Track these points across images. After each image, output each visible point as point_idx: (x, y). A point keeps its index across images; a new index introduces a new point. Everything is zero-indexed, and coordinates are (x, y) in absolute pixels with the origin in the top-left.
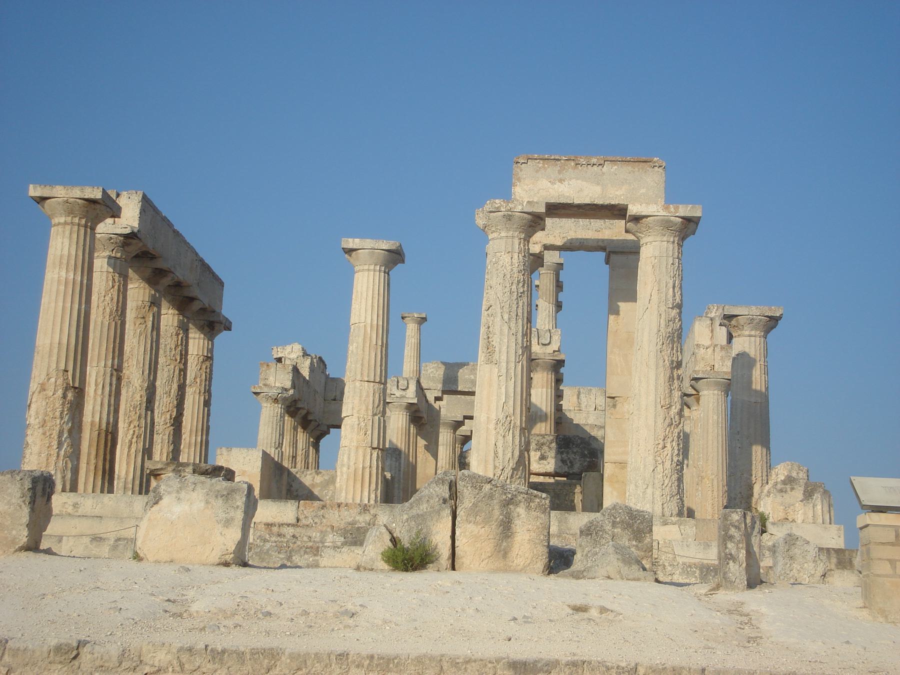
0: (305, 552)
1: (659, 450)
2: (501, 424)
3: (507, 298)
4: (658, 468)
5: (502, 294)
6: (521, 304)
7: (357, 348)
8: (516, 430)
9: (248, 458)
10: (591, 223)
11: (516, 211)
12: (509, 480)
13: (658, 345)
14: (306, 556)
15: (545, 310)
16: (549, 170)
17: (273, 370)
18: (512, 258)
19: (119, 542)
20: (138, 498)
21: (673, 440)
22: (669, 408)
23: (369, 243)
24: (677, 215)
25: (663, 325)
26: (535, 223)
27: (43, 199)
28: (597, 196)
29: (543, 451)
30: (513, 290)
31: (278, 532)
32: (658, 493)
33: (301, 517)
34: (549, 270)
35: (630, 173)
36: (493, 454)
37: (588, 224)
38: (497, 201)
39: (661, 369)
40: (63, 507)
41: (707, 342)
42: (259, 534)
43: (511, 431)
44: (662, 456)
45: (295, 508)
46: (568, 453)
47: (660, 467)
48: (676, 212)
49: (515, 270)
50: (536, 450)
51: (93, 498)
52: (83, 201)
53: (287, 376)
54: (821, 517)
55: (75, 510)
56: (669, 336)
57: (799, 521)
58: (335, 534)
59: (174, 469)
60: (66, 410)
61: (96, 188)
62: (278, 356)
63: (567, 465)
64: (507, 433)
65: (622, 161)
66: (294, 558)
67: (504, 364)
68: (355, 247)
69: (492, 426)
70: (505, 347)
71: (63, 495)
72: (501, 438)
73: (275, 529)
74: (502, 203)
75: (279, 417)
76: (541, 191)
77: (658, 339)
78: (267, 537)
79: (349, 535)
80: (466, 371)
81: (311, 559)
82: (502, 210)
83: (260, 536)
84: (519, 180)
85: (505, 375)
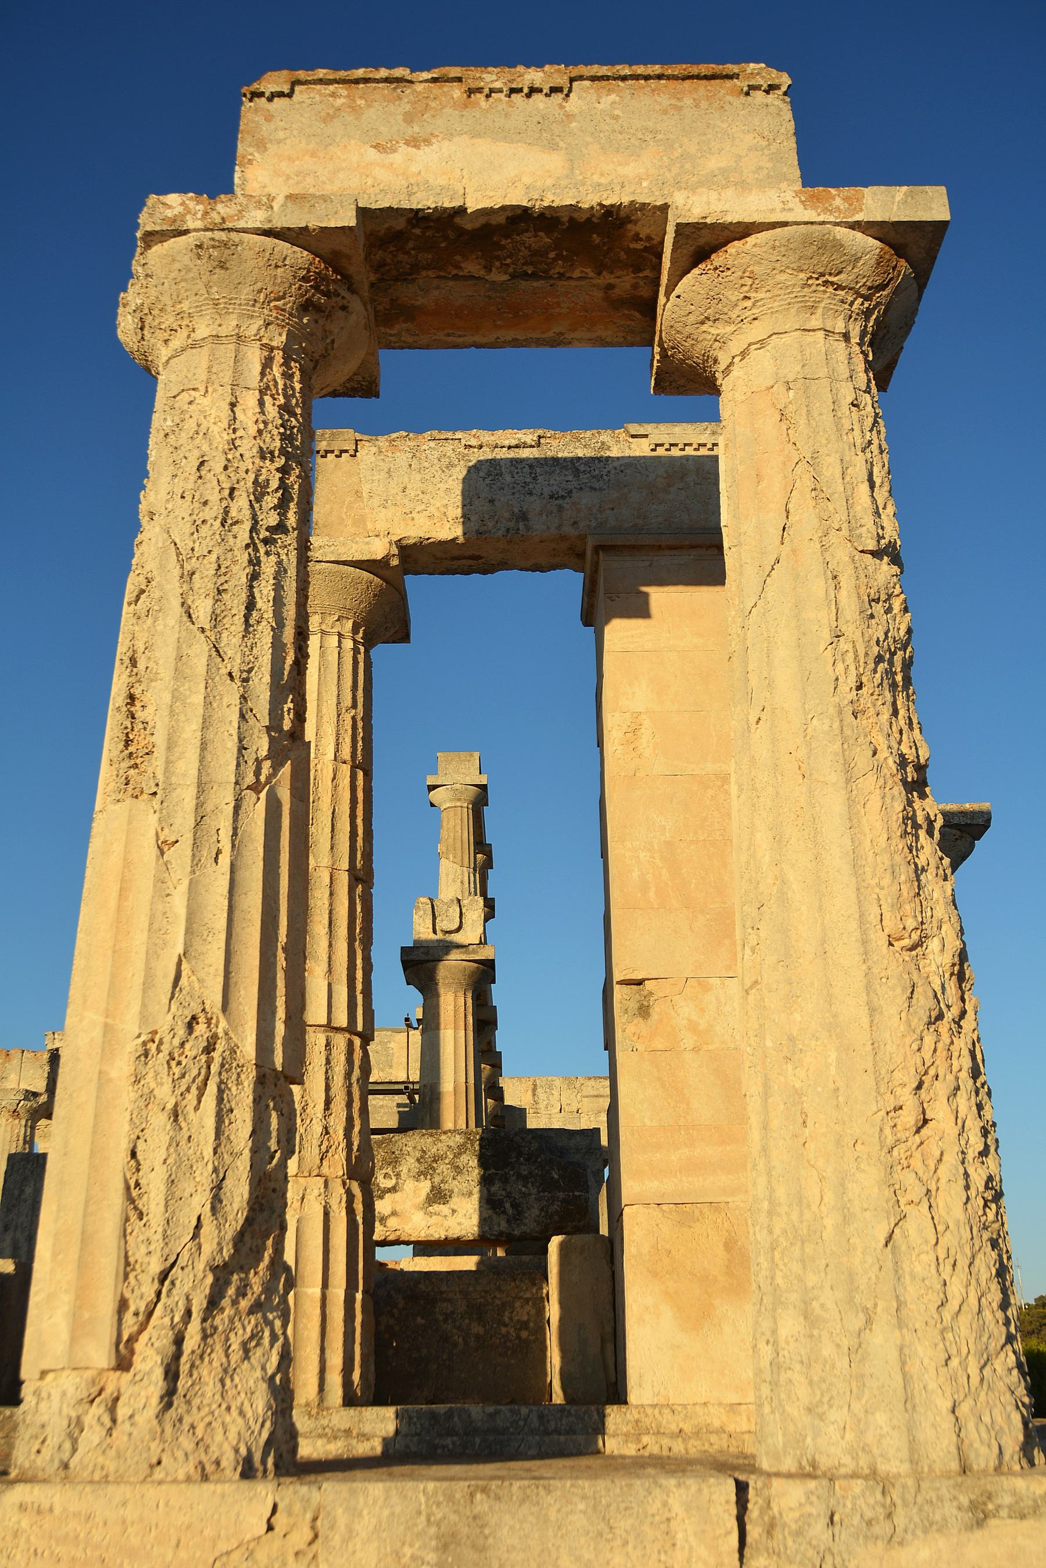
1: (902, 1135)
2: (163, 1056)
4: (910, 1226)
5: (188, 528)
6: (268, 567)
8: (239, 1083)
10: (535, 478)
11: (241, 224)
18: (233, 405)
26: (327, 294)
28: (549, 182)
29: (437, 1179)
30: (233, 513)
34: (459, 800)
35: (665, 112)
36: (116, 1199)
39: (870, 782)
43: (212, 1088)
44: (916, 1163)
46: (505, 1180)
49: (248, 447)
53: (41, 1071)
56: (879, 659)
62: (55, 1047)
63: (504, 1212)
67: (188, 796)
69: (122, 1067)
70: (195, 725)
72: (159, 1121)
75: (21, 1142)
76: (341, 175)
77: (840, 667)
84: (261, 145)
85: (189, 836)
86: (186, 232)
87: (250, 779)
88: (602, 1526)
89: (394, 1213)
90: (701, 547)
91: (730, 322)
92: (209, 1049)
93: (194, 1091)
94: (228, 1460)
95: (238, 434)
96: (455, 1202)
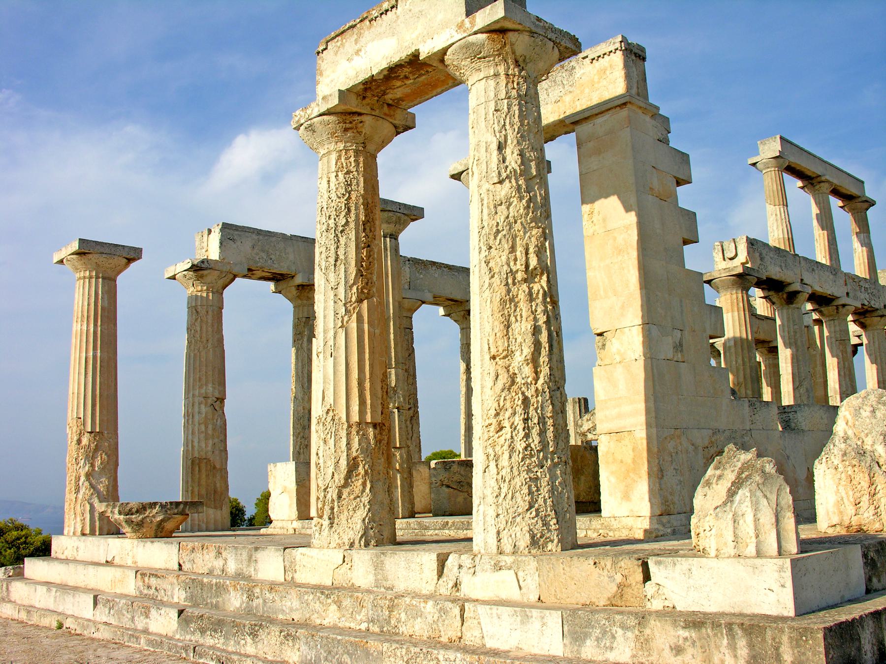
1: (491, 435)
3: (324, 239)
10: (548, 95)
11: (313, 116)
12: (336, 504)
13: (483, 251)
15: (772, 215)
18: (329, 181)
21: (515, 413)
22: (509, 354)
24: (475, 29)
25: (485, 217)
26: (351, 123)
32: (491, 512)
33: (181, 562)
34: (768, 168)
37: (546, 97)
38: (297, 113)
47: (493, 464)
48: (473, 26)
54: (754, 540)
57: (713, 553)
60: (80, 455)
64: (329, 436)
72: (322, 443)
73: (146, 579)
74: (301, 113)
82: (302, 121)
86: (302, 124)
87: (340, 324)
88: (407, 565)
90: (612, 108)
92: (333, 420)
93: (330, 434)
94: (346, 541)
95: (331, 192)
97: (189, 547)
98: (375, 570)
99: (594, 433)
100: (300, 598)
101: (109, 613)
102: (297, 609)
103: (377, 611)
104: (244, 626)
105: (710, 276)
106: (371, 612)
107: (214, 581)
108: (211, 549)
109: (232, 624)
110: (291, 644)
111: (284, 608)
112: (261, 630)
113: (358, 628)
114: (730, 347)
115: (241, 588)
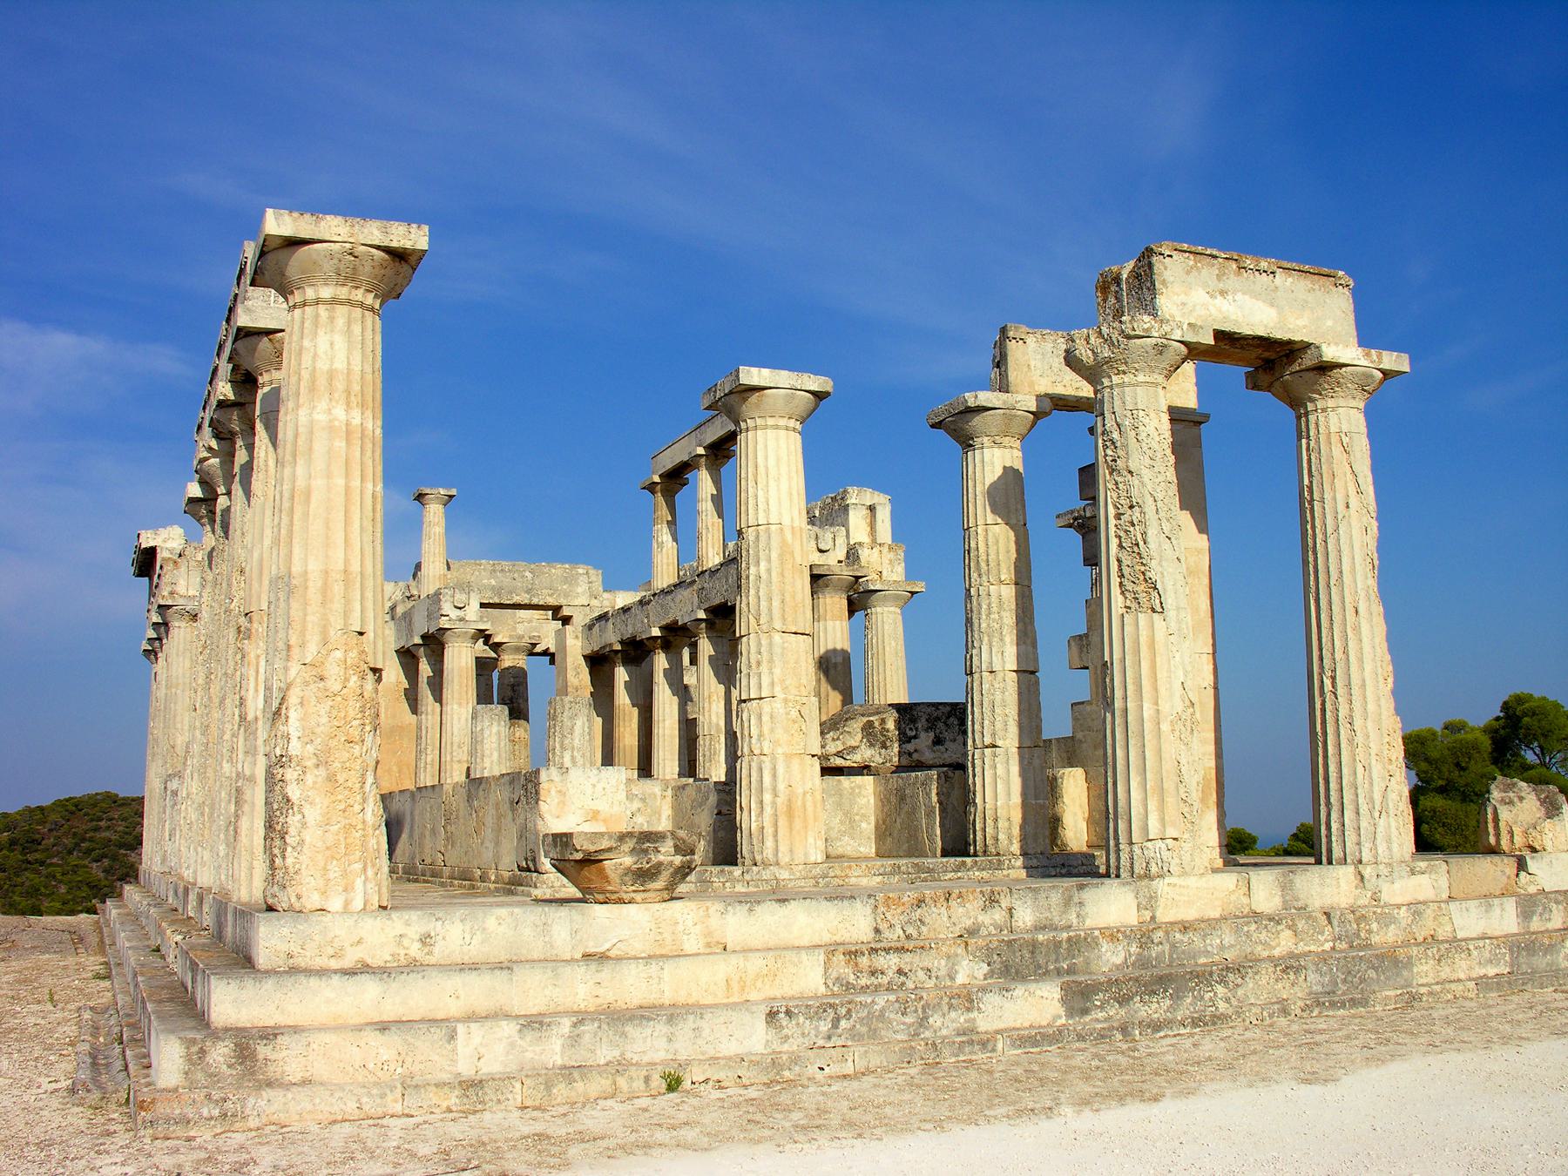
0: (951, 1006)
7: (769, 571)
9: (599, 787)
14: (953, 1014)
16: (1204, 272)
17: (183, 569)
19: (582, 1028)
20: (558, 915)
23: (784, 378)
27: (294, 243)
29: (938, 731)
31: (870, 967)
33: (883, 926)
40: (399, 944)
41: (866, 539)
42: (835, 975)
45: (869, 910)
50: (926, 730)
51: (462, 921)
52: (382, 254)
55: (426, 950)
58: (971, 958)
59: (634, 848)
61: (414, 226)
65: (1299, 271)
66: (931, 1020)
68: (763, 384)
71: (395, 918)
73: (864, 961)
74: (1153, 322)
78: (852, 978)
79: (995, 957)
80: (483, 573)
81: (962, 1020)
83: (838, 979)
89: (916, 751)
91: (1321, 394)
96: (948, 744)
97: (906, 899)
98: (1283, 891)
99: (848, 757)
100: (1237, 930)
101: (836, 1023)
102: (1232, 946)
103: (1345, 926)
104: (1211, 974)
105: (828, 570)
106: (1337, 929)
107: (1065, 935)
108: (971, 898)
109: (1188, 977)
110: (1292, 977)
111: (1209, 948)
112: (1230, 975)
113: (1320, 950)
114: (835, 663)
115: (1126, 937)
